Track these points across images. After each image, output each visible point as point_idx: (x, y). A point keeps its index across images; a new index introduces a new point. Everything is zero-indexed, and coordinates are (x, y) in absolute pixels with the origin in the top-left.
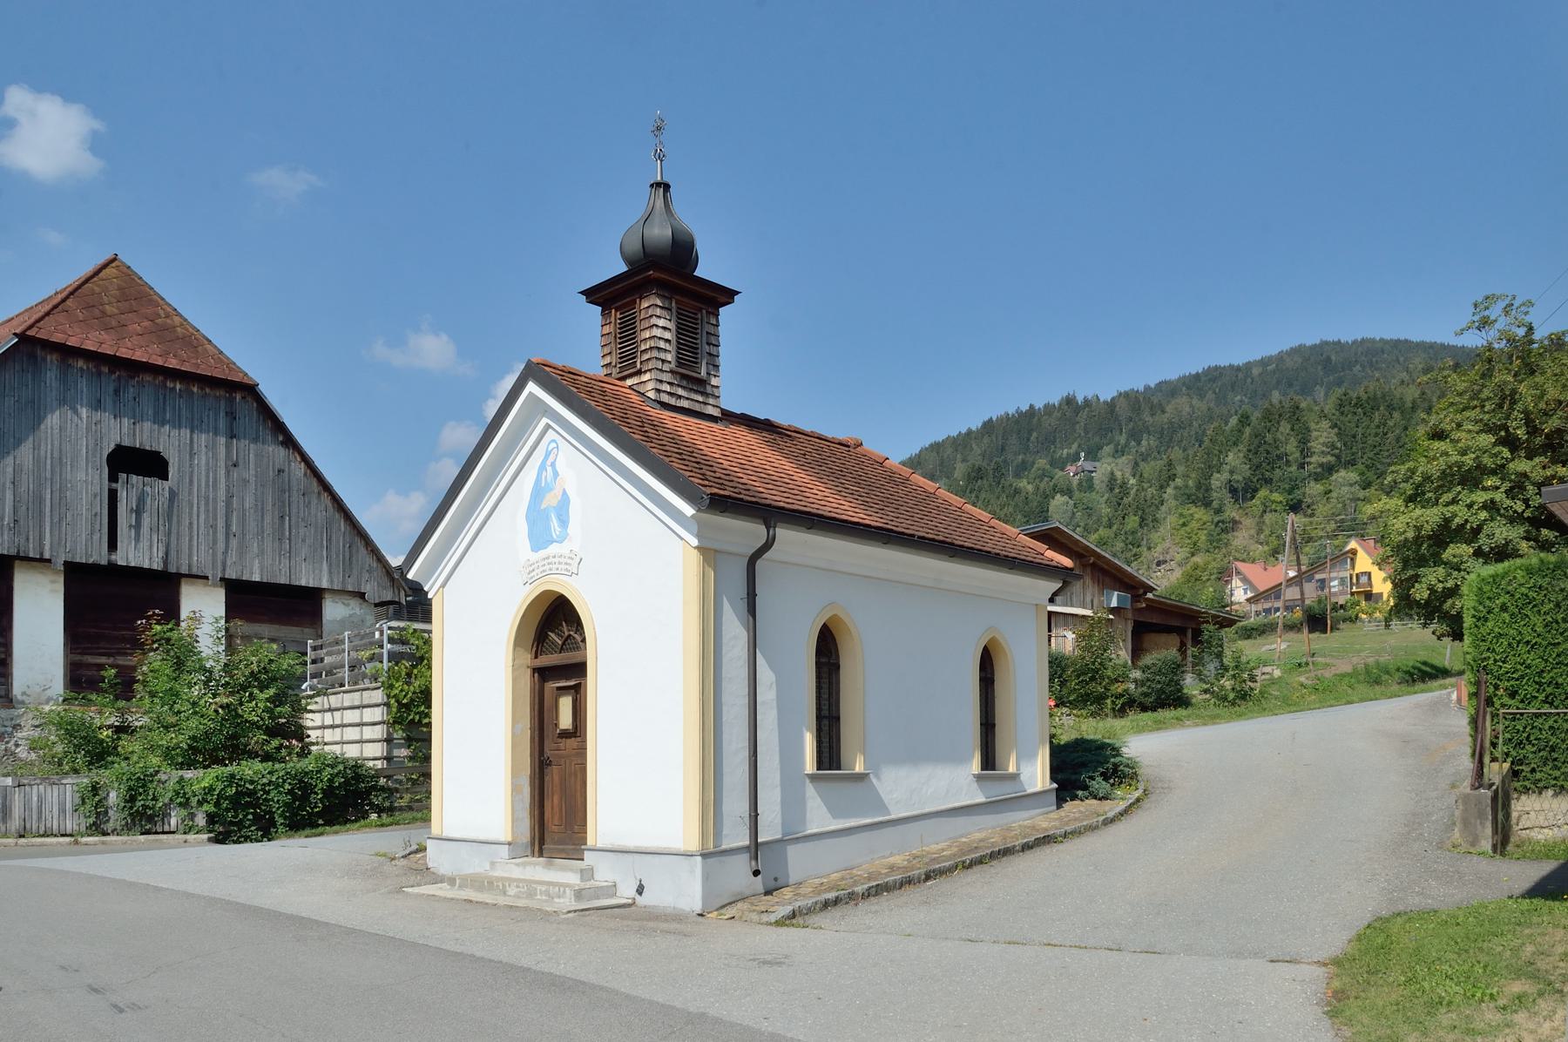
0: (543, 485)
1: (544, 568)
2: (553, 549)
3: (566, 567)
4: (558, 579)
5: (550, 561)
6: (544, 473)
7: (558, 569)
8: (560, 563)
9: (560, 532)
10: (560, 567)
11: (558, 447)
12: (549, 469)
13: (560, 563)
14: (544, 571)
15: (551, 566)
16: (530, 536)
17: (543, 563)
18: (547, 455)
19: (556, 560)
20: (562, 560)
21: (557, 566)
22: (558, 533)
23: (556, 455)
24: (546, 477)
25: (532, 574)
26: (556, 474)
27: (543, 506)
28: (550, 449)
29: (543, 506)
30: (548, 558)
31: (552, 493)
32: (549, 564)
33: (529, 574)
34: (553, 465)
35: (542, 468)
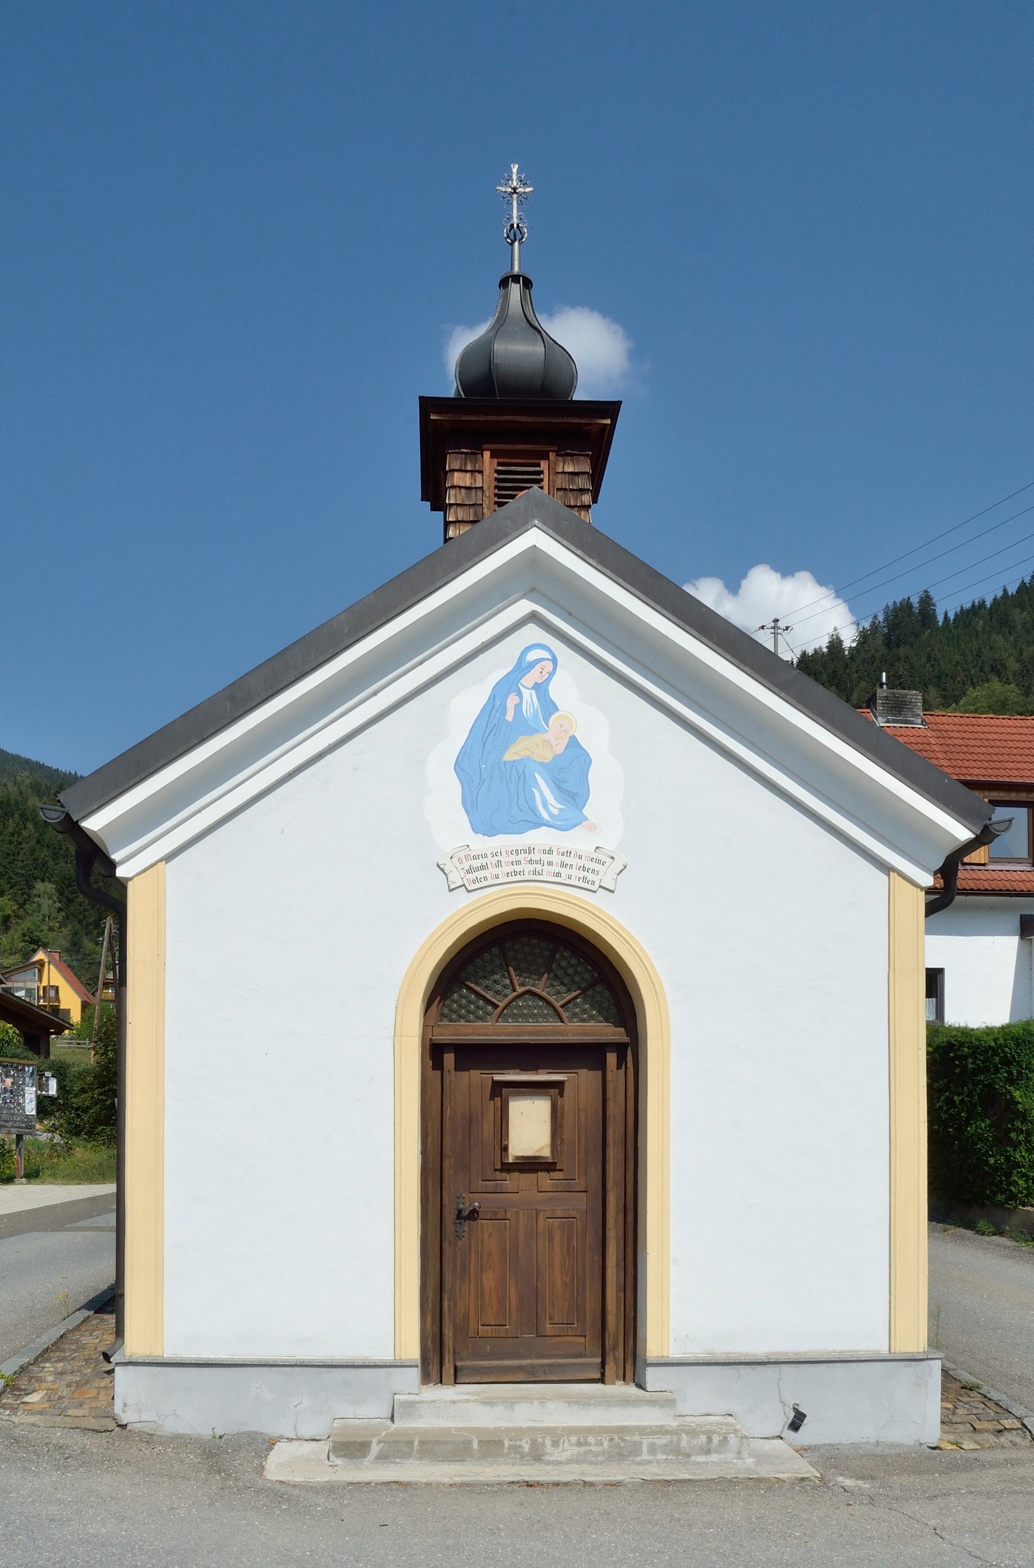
0: (510, 717)
1: (518, 868)
2: (538, 837)
3: (582, 874)
4: (561, 893)
5: (535, 857)
6: (512, 701)
7: (558, 875)
8: (563, 865)
9: (561, 810)
10: (564, 871)
11: (554, 660)
12: (529, 697)
13: (563, 865)
14: (516, 873)
15: (539, 867)
16: (470, 804)
17: (513, 858)
18: (522, 667)
19: (555, 858)
20: (568, 860)
21: (556, 869)
22: (555, 812)
23: (551, 675)
24: (518, 707)
25: (480, 874)
26: (549, 707)
27: (509, 756)
28: (532, 656)
29: (509, 756)
30: (530, 851)
31: (537, 738)
32: (531, 862)
33: (468, 872)
34: (541, 688)
35: (509, 685)
